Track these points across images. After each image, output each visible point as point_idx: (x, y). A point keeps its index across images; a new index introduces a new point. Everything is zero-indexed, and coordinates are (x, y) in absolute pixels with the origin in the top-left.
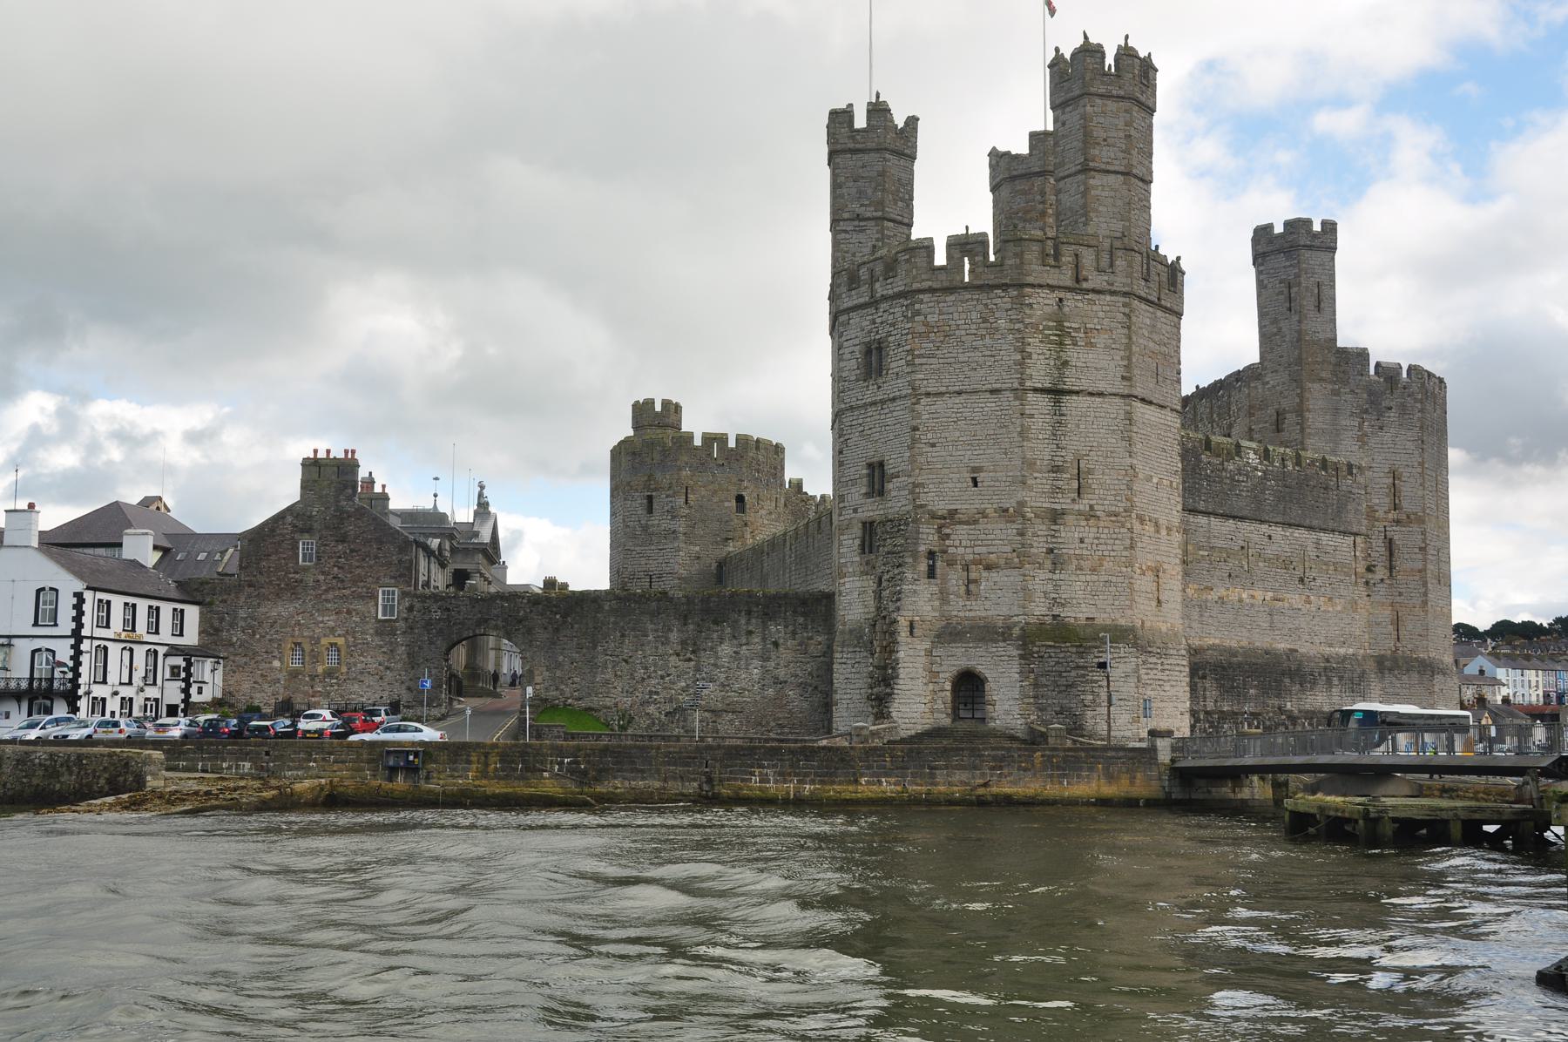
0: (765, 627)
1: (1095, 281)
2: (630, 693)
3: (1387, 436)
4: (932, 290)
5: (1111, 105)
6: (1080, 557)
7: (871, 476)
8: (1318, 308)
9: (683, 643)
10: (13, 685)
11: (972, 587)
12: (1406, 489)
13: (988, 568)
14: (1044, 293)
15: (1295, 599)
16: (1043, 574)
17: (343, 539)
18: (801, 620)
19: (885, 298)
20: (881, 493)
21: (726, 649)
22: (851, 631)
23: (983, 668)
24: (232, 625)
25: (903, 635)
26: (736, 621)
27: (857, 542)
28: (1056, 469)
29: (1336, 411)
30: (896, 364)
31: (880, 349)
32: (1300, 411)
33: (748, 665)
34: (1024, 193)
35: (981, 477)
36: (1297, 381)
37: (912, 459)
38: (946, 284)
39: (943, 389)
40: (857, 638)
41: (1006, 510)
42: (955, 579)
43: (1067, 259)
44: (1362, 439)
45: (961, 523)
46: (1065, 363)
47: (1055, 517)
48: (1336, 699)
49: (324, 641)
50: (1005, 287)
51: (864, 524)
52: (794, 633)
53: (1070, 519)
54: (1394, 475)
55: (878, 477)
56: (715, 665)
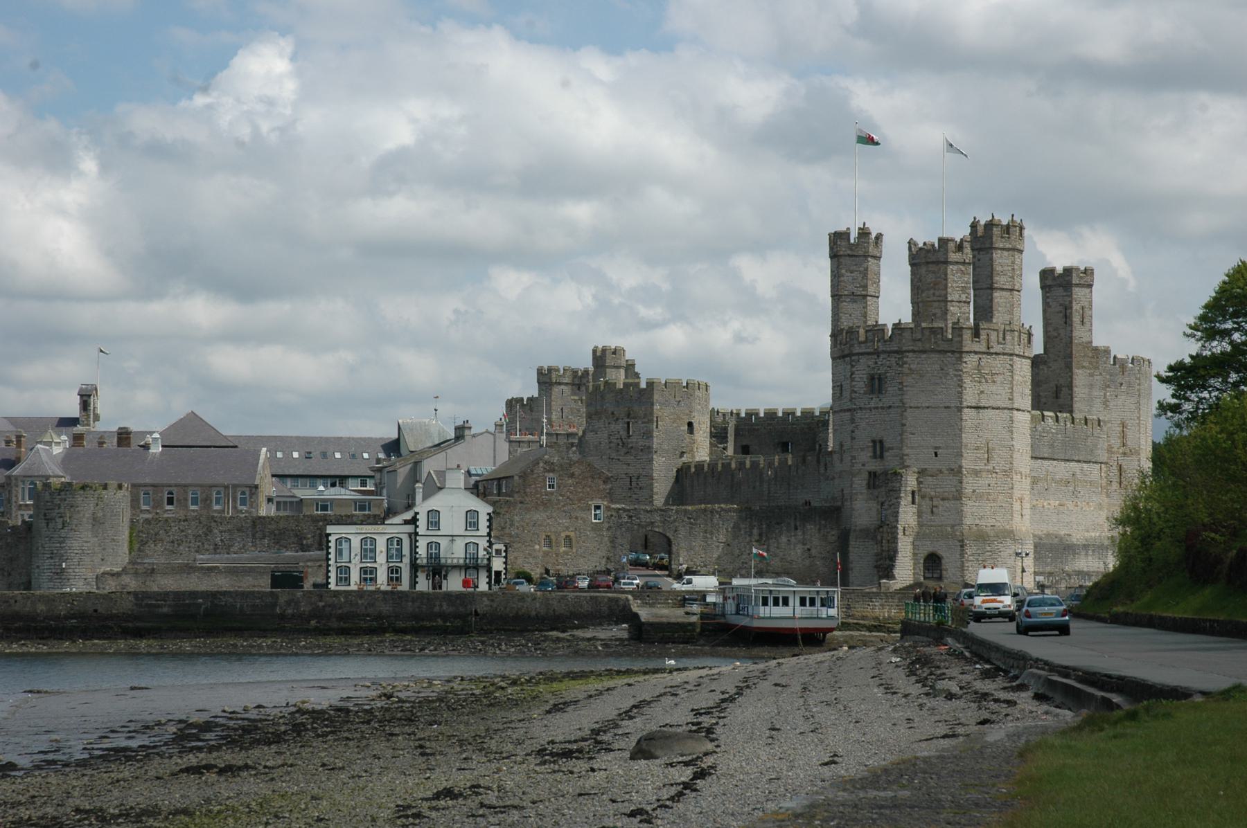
1: (997, 348)
3: (1120, 401)
4: (914, 351)
5: (1006, 253)
6: (989, 494)
7: (874, 447)
8: (1083, 323)
9: (760, 535)
10: (455, 561)
12: (1129, 433)
13: (943, 499)
14: (972, 355)
15: (1070, 505)
16: (970, 503)
17: (572, 475)
19: (884, 352)
20: (882, 457)
21: (784, 539)
23: (940, 552)
24: (512, 525)
25: (900, 535)
27: (865, 482)
28: (977, 448)
29: (1091, 386)
30: (891, 388)
31: (880, 379)
32: (1070, 387)
34: (934, 272)
35: (939, 451)
36: (1069, 367)
37: (902, 441)
40: (867, 534)
42: (926, 505)
43: (983, 336)
44: (1106, 403)
46: (982, 392)
47: (977, 473)
48: (1090, 564)
49: (563, 535)
50: (953, 352)
53: (984, 474)
54: (1123, 425)
55: (879, 449)
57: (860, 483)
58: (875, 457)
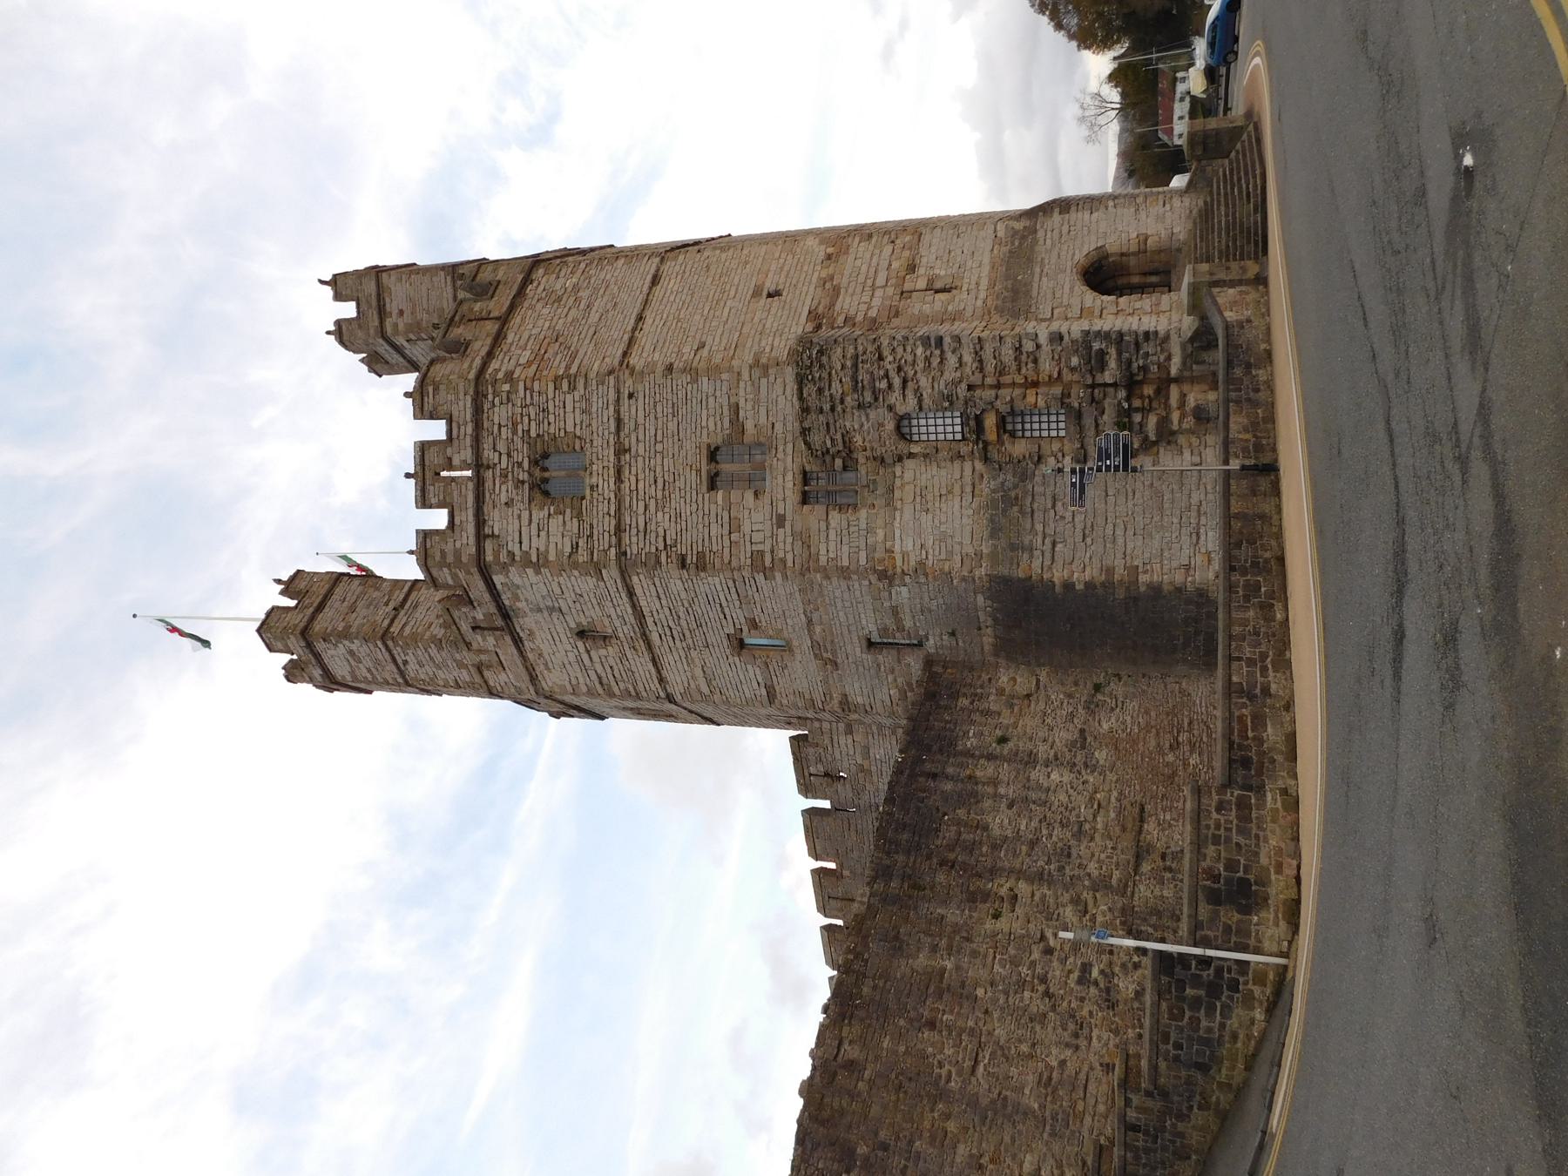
0: (968, 754)
2: (1081, 1028)
4: (490, 355)
11: (938, 285)
13: (912, 268)
18: (964, 702)
21: (1000, 822)
22: (994, 533)
26: (946, 797)
27: (835, 517)
33: (1039, 787)
35: (770, 285)
37: (714, 371)
38: (489, 341)
39: (626, 337)
41: (829, 257)
45: (832, 305)
51: (805, 499)
52: (987, 713)
56: (1033, 844)
57: (838, 536)
58: (755, 482)
